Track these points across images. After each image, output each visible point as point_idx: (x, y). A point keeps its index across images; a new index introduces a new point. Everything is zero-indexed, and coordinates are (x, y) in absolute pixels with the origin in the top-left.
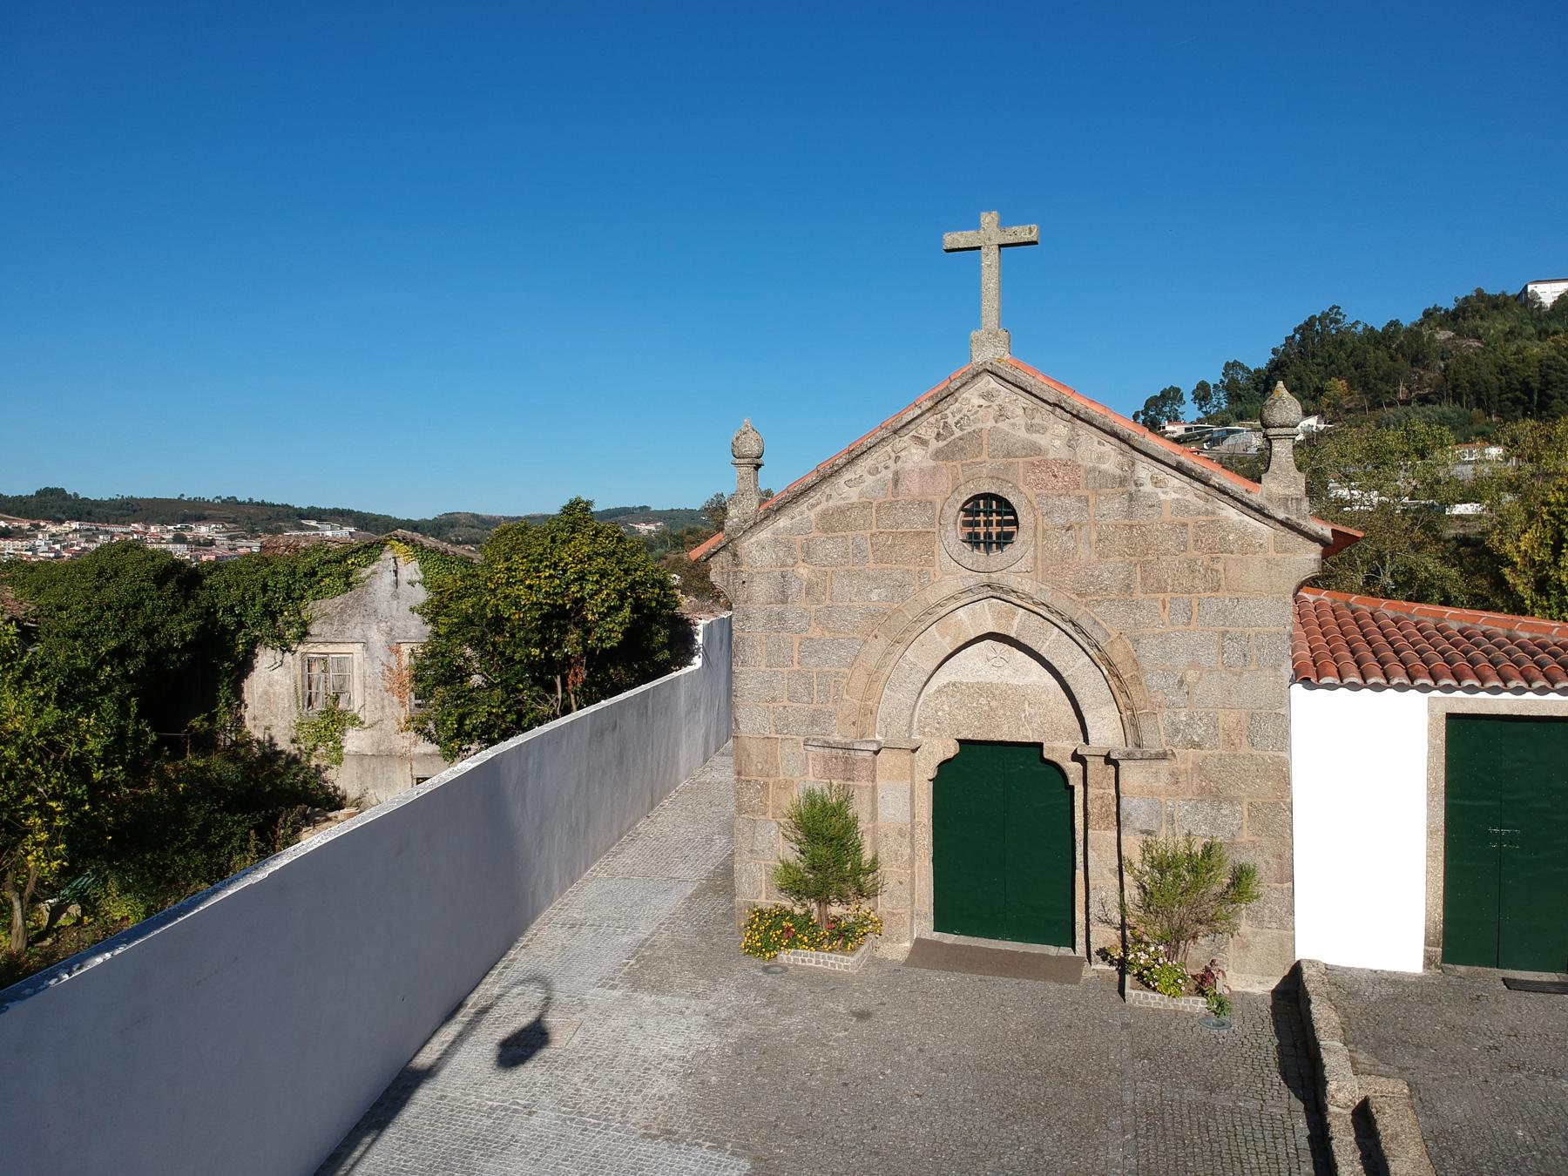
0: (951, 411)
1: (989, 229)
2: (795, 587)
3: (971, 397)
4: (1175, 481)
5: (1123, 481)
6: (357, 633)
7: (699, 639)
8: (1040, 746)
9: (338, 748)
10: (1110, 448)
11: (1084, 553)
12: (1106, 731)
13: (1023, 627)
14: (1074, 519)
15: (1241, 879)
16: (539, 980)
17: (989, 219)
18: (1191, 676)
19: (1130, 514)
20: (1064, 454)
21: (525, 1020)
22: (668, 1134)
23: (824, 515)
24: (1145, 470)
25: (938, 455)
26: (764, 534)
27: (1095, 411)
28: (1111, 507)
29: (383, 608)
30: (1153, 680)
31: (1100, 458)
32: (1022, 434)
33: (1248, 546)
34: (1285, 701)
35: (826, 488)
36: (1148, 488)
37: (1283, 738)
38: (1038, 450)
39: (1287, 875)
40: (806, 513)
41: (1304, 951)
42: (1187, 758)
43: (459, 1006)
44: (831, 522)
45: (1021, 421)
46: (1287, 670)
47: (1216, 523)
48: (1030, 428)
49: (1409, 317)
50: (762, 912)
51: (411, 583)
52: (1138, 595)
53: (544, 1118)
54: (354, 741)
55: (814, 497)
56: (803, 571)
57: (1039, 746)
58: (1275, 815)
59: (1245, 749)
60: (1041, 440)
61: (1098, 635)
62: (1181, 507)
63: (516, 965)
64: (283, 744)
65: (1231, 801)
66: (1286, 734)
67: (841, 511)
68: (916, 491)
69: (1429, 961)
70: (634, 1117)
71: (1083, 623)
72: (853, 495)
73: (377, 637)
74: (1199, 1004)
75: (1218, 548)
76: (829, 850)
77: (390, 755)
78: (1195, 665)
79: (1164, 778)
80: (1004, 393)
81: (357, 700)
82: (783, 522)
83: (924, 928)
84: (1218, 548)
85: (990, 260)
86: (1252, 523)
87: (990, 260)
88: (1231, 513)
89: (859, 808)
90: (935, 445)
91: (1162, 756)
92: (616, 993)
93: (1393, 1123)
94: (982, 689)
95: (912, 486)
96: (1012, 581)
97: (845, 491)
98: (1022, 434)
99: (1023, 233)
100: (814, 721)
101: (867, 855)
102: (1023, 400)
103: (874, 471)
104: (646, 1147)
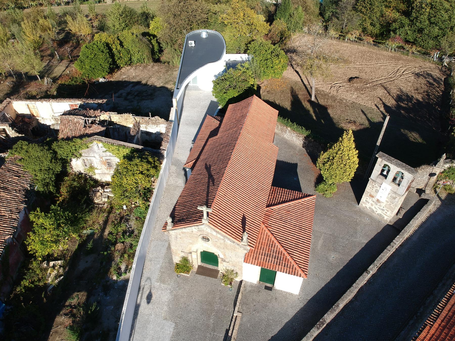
6: (92, 155)
7: (165, 156)
9: (94, 172)
15: (237, 273)
16: (149, 278)
21: (148, 292)
22: (166, 319)
24: (226, 240)
26: (174, 231)
28: (222, 241)
29: (97, 151)
39: (242, 273)
41: (243, 278)
43: (139, 288)
44: (182, 233)
46: (243, 259)
50: (177, 264)
51: (102, 147)
53: (153, 316)
54: (96, 171)
56: (179, 236)
58: (241, 269)
63: (146, 287)
64: (82, 172)
70: (163, 315)
73: (97, 156)
74: (229, 286)
76: (185, 260)
77: (105, 173)
81: (96, 166)
82: (176, 231)
83: (200, 263)
89: (190, 258)
91: (228, 262)
92: (158, 284)
93: (238, 319)
101: (191, 262)
104: (164, 322)
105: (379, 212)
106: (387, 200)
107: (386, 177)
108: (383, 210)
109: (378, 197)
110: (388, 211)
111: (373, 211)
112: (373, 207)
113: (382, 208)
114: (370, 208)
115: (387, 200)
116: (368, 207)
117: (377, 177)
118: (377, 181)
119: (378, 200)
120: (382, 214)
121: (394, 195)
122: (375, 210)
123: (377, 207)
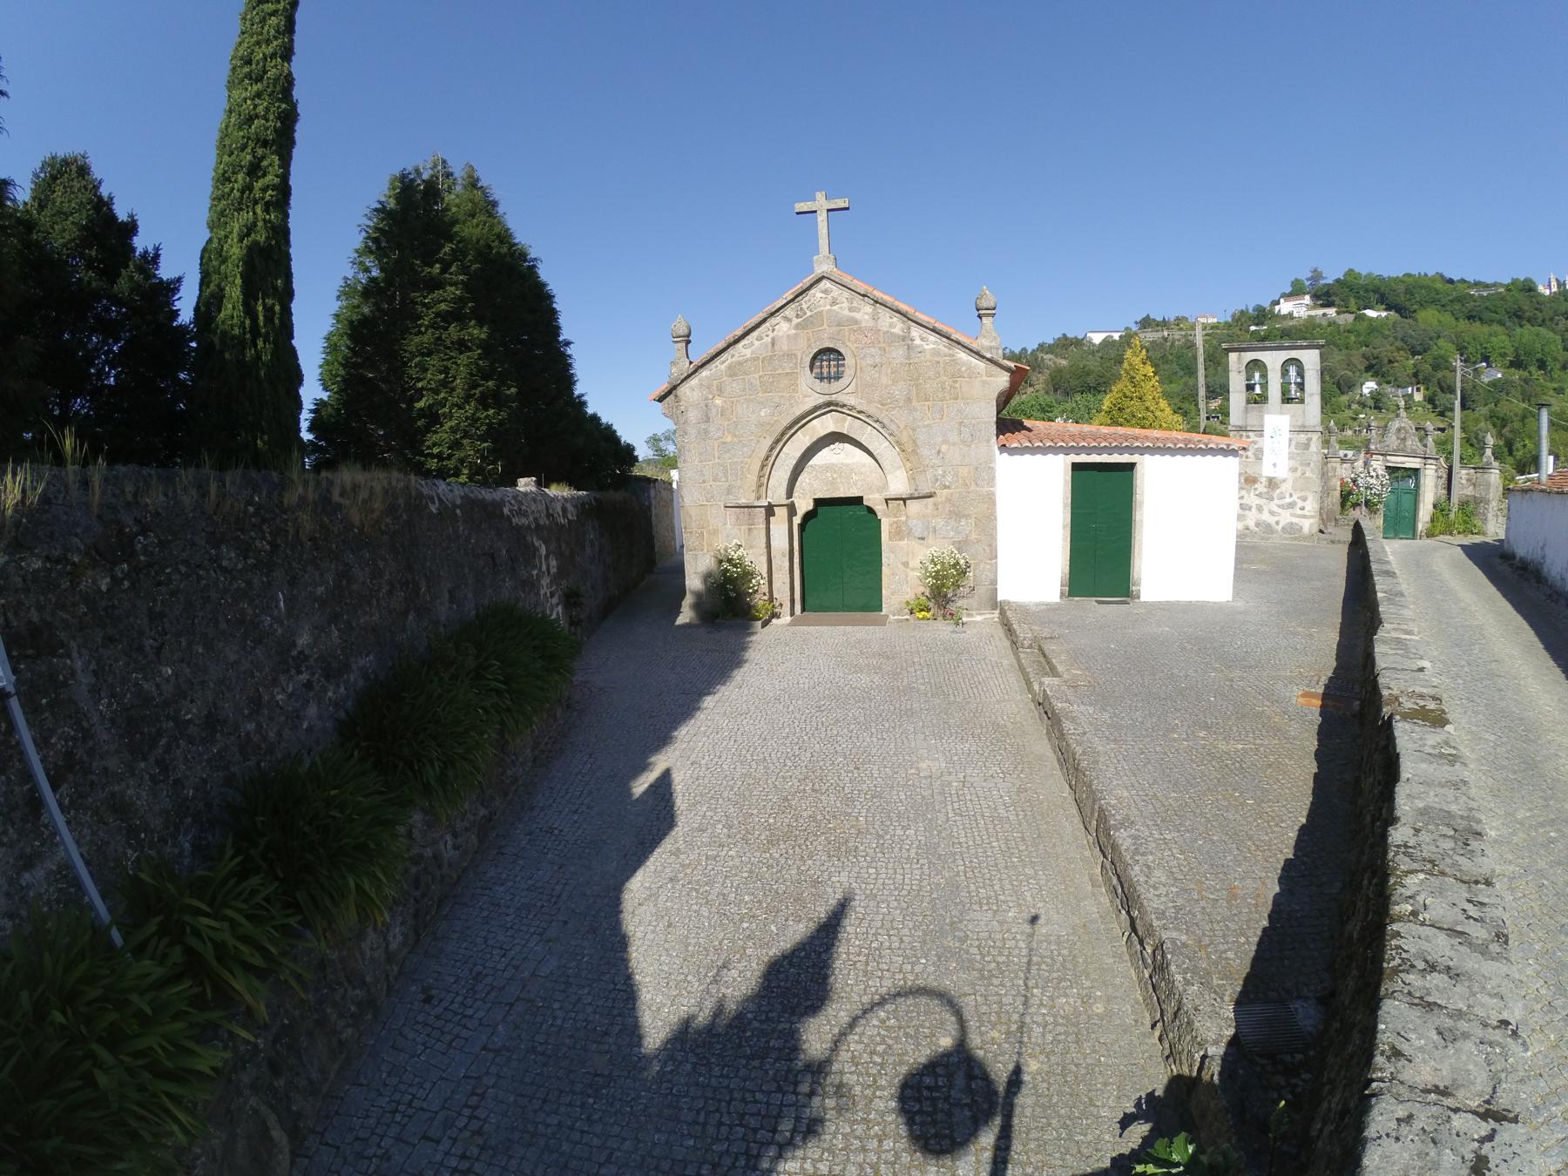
0: (805, 302)
1: (821, 203)
2: (714, 411)
3: (816, 293)
4: (933, 337)
5: (904, 339)
8: (861, 498)
10: (896, 319)
11: (885, 380)
12: (898, 484)
13: (851, 427)
14: (878, 360)
17: (820, 196)
18: (944, 448)
19: (909, 358)
20: (871, 324)
23: (730, 367)
24: (916, 332)
25: (797, 327)
27: (887, 298)
28: (898, 353)
30: (924, 451)
31: (891, 325)
32: (846, 312)
33: (972, 374)
34: (991, 460)
35: (731, 351)
36: (918, 342)
37: (992, 481)
38: (856, 322)
40: (720, 365)
42: (942, 494)
45: (846, 305)
47: (955, 362)
48: (850, 309)
49: (1031, 346)
52: (914, 403)
55: (724, 356)
56: (718, 401)
57: (861, 498)
59: (973, 488)
60: (857, 316)
61: (893, 427)
62: (936, 353)
65: (967, 517)
66: (993, 478)
67: (740, 363)
68: (785, 348)
69: (1062, 594)
71: (886, 421)
72: (748, 353)
75: (956, 376)
78: (944, 442)
79: (930, 507)
80: (836, 291)
84: (956, 376)
85: (822, 217)
86: (974, 361)
87: (822, 217)
88: (963, 355)
90: (796, 321)
94: (829, 468)
95: (784, 346)
96: (841, 398)
97: (743, 350)
98: (846, 312)
99: (841, 203)
100: (729, 492)
102: (847, 294)
103: (759, 338)
105: (1286, 518)
106: (1293, 463)
107: (1262, 399)
108: (1292, 505)
109: (1267, 471)
110: (1304, 499)
111: (1268, 528)
112: (1266, 517)
113: (1288, 500)
114: (1257, 525)
115: (1293, 463)
116: (1251, 524)
117: (1246, 411)
118: (1250, 422)
119: (1272, 483)
120: (1295, 520)
121: (1303, 436)
122: (1271, 520)
123: (1273, 506)
